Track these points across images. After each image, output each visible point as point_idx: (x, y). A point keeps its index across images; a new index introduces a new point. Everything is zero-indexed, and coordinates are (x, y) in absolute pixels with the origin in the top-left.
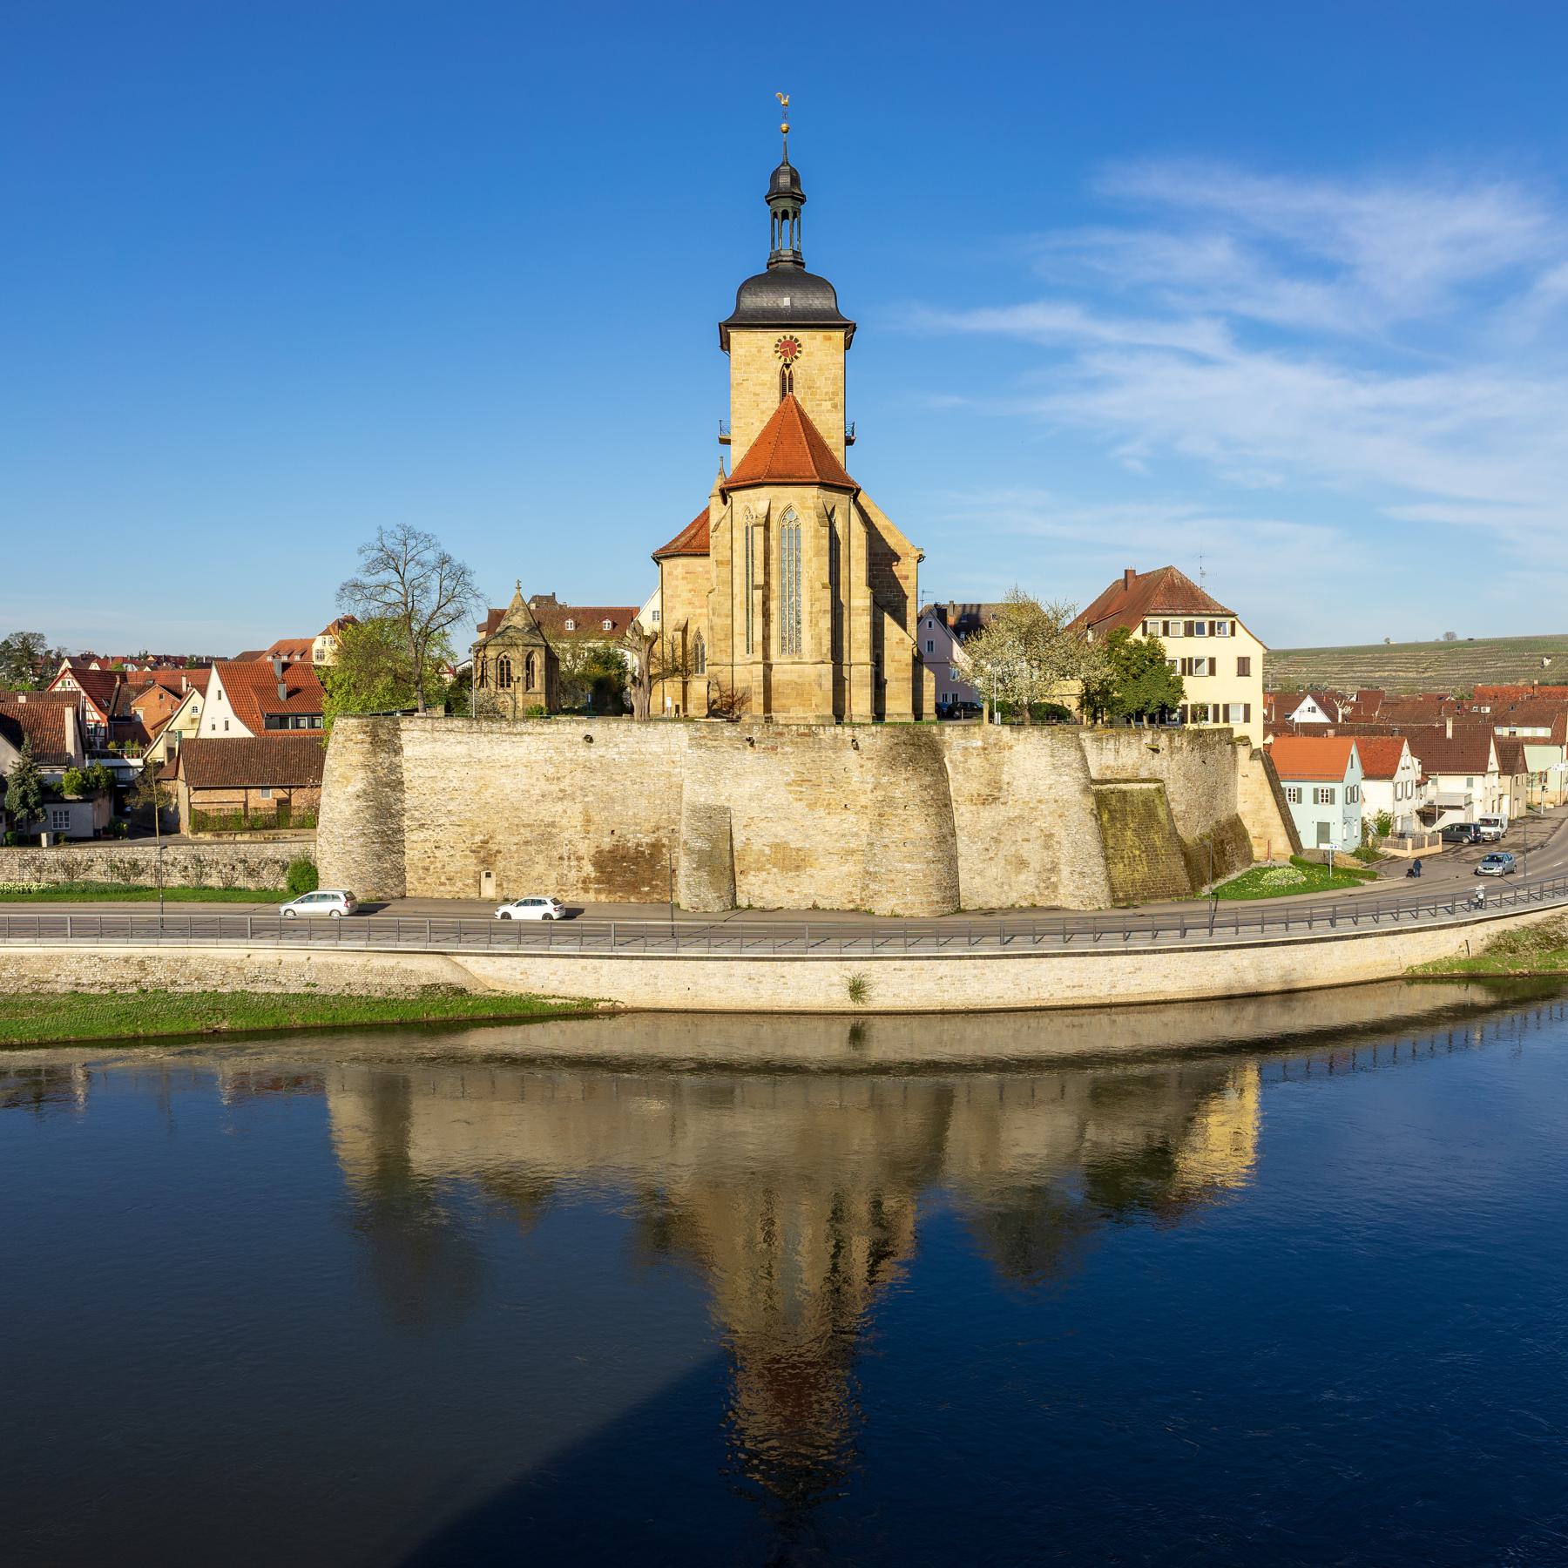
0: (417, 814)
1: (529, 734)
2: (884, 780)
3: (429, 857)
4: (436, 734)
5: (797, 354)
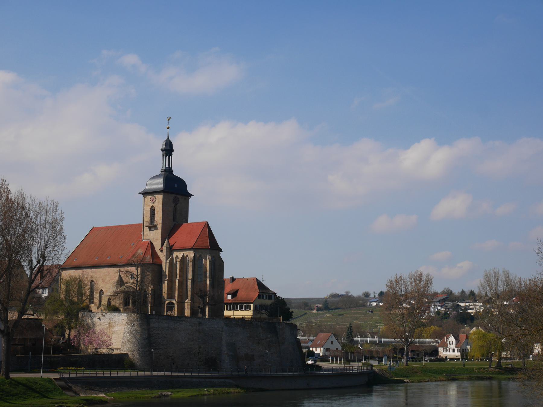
0: (154, 345)
1: (185, 321)
2: (269, 336)
3: (158, 358)
4: (159, 320)
5: (178, 203)
